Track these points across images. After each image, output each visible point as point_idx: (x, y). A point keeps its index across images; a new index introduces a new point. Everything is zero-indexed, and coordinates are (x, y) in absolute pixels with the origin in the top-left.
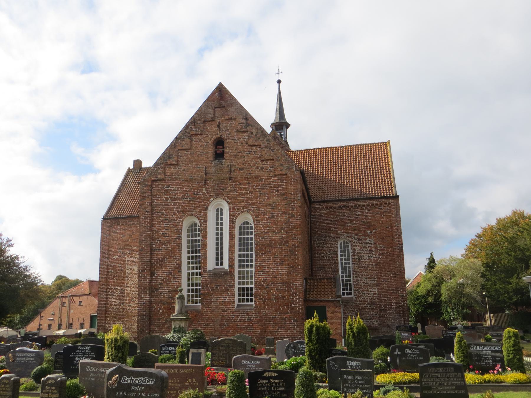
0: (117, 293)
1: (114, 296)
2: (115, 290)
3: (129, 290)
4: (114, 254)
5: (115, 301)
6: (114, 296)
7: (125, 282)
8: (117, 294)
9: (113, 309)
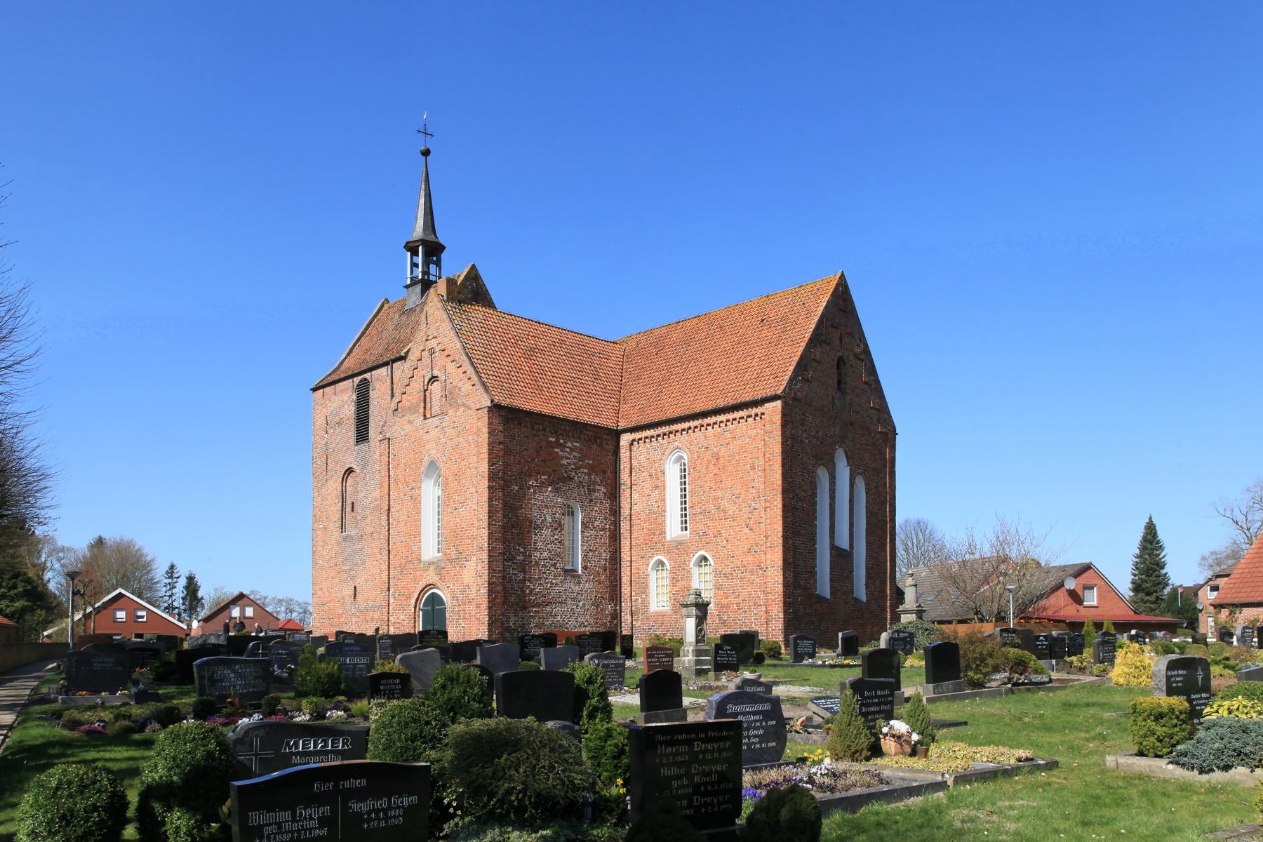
0: (518, 558)
3: (538, 554)
5: (515, 574)
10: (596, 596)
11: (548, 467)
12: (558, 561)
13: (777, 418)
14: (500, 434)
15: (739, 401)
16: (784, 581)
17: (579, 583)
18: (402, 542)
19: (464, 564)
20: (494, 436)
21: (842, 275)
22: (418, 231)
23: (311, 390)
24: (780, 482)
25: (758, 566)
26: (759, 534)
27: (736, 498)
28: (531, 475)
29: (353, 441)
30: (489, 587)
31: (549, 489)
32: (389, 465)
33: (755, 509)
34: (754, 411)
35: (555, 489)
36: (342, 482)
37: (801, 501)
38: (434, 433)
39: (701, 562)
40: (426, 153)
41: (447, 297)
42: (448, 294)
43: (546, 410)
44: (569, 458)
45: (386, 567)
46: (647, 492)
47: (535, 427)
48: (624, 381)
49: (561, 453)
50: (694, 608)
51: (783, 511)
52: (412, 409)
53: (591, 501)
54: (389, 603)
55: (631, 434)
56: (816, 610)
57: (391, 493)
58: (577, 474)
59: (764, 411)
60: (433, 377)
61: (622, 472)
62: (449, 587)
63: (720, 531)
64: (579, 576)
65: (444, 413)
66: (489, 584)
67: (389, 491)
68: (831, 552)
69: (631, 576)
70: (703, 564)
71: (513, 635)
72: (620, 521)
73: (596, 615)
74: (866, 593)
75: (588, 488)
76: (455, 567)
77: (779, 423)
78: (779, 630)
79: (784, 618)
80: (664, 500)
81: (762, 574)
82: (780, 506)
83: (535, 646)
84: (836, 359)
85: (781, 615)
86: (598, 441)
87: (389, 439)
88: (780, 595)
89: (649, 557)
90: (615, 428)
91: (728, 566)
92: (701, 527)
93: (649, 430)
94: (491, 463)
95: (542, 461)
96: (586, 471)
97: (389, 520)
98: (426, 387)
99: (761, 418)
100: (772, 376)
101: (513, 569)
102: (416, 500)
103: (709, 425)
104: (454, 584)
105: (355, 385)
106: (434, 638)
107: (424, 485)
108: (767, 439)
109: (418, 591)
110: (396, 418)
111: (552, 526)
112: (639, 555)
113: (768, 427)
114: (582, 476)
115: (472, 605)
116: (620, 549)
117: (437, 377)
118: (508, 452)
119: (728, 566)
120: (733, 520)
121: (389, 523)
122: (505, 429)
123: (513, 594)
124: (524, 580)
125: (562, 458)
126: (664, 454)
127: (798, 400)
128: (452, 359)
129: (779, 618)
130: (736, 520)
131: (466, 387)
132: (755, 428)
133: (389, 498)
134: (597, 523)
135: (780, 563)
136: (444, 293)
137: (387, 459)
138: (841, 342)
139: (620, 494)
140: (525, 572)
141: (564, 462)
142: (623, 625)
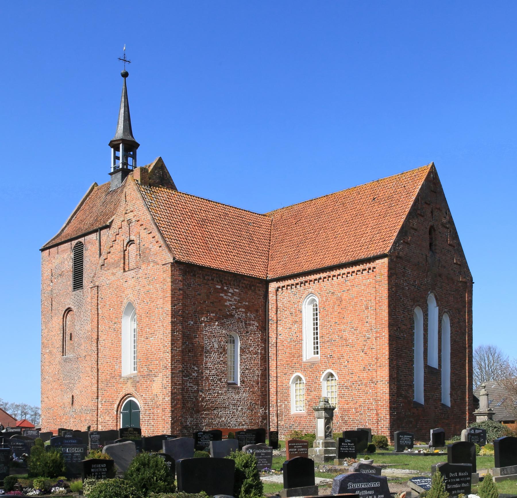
0: (193, 374)
1: (190, 378)
2: (192, 370)
4: (188, 318)
6: (190, 378)
7: (203, 361)
8: (194, 376)
9: (190, 397)
10: (251, 403)
11: (215, 307)
12: (223, 376)
13: (385, 271)
14: (180, 283)
15: (357, 258)
16: (390, 391)
17: (238, 393)
18: (107, 363)
19: (153, 379)
20: (176, 284)
21: (433, 165)
22: (119, 132)
23: (40, 250)
24: (387, 319)
25: (371, 380)
26: (372, 357)
27: (355, 330)
28: (203, 313)
29: (71, 288)
30: (172, 396)
31: (216, 324)
32: (98, 305)
33: (368, 338)
34: (368, 265)
35: (221, 323)
36: (63, 318)
37: (402, 333)
38: (131, 282)
39: (329, 377)
40: (125, 75)
41: (141, 181)
42: (141, 179)
43: (214, 265)
44: (231, 301)
45: (96, 381)
46: (289, 325)
47: (206, 278)
48: (271, 243)
49: (225, 297)
50: (324, 411)
51: (389, 340)
52: (115, 265)
53: (247, 332)
54: (98, 408)
55: (277, 282)
56: (414, 413)
57: (99, 327)
58: (237, 313)
59: (375, 266)
60: (130, 241)
61: (270, 311)
63: (342, 354)
64: (238, 388)
65: (139, 268)
66: (172, 394)
67: (98, 325)
68: (425, 371)
69: (277, 388)
70: (330, 379)
71: (189, 431)
72: (268, 347)
73: (251, 417)
74: (451, 401)
75: (245, 323)
76: (147, 381)
77: (386, 275)
78: (386, 427)
79: (390, 419)
80: (301, 332)
81: (374, 386)
82: (387, 336)
83: (205, 439)
84: (428, 227)
85: (388, 417)
86: (252, 288)
87: (98, 286)
88: (387, 402)
89: (290, 374)
90: (265, 278)
91: (349, 380)
92: (329, 351)
93: (290, 280)
94: (173, 305)
95: (211, 303)
96: (244, 310)
97: (97, 346)
98: (125, 248)
99: (373, 271)
100: (381, 240)
101: (190, 382)
102: (118, 332)
103: (334, 276)
104: (146, 394)
105: (73, 247)
106: (131, 434)
107: (123, 321)
108: (377, 286)
109: (119, 399)
110: (103, 271)
111: (219, 351)
112: (283, 373)
113: (378, 278)
114: (240, 314)
115: (159, 409)
116: (269, 368)
117: (133, 241)
118: (185, 296)
119: (349, 380)
120: (352, 347)
121: (98, 349)
122: (183, 280)
123: (190, 401)
124: (198, 391)
125: (226, 300)
126: (301, 298)
127: (400, 258)
128: (145, 228)
129: (386, 419)
130: (355, 346)
131: (155, 248)
132: (368, 279)
133: (98, 330)
134: (251, 349)
135: (387, 378)
136: (139, 179)
137: (96, 302)
138: (432, 215)
139: (268, 327)
140: (198, 385)
141: (228, 303)
142: (271, 424)
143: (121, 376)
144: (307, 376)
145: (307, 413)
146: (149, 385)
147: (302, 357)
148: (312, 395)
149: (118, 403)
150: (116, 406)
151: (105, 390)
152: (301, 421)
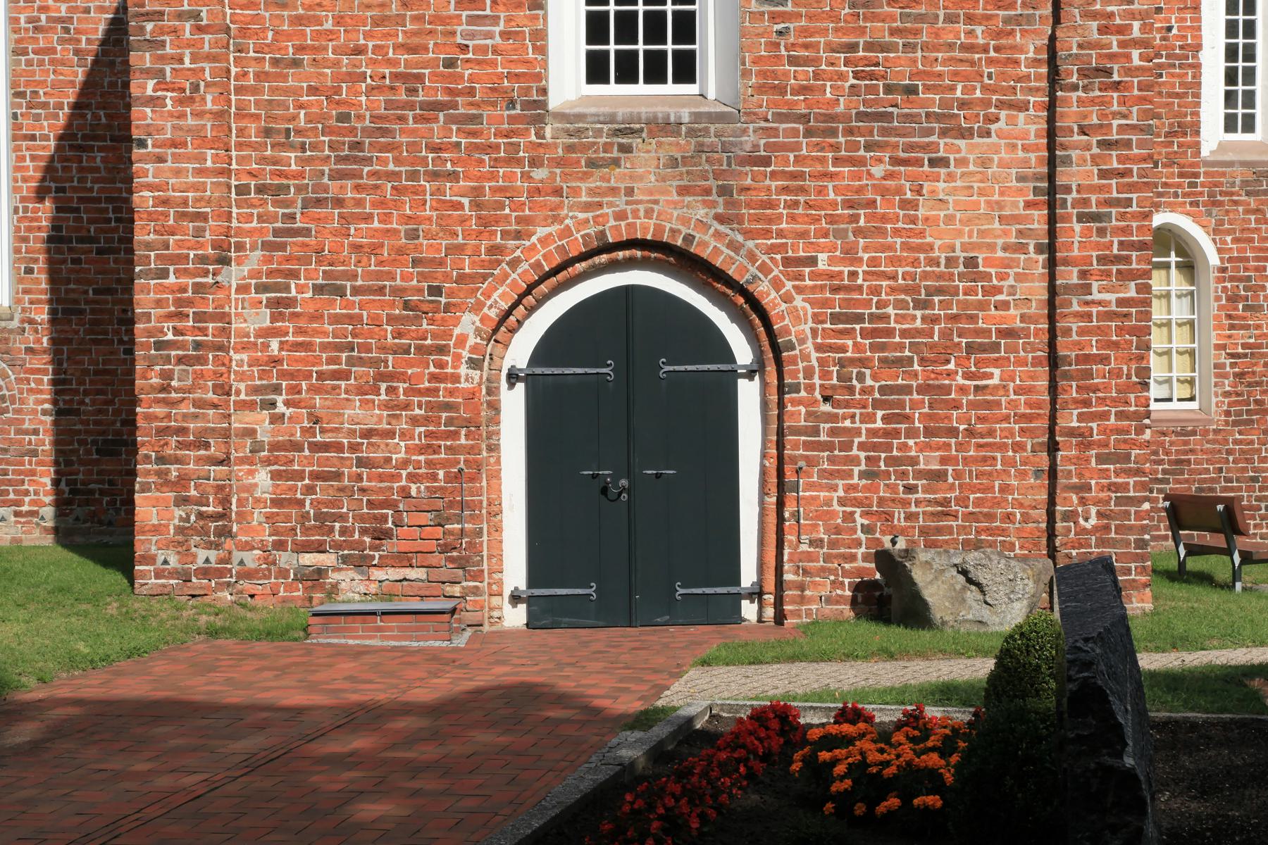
62: (813, 261)
109: (519, 277)
143: (543, 105)
144: (1228, 232)
145: (1228, 413)
146: (884, 192)
147: (1198, 133)
148: (1258, 327)
149: (500, 299)
150: (468, 324)
151: (319, 202)
152: (1186, 452)
